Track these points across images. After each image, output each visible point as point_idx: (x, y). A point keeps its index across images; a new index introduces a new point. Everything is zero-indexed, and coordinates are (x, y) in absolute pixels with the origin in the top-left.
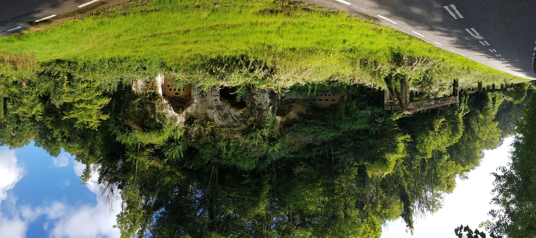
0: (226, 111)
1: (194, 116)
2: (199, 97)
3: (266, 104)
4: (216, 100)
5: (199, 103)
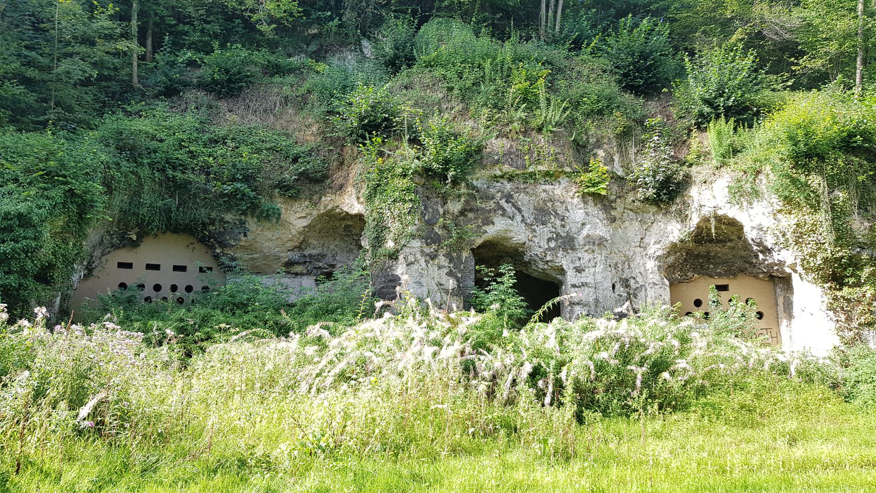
0: (544, 232)
3: (411, 259)
4: (579, 270)
5: (638, 259)
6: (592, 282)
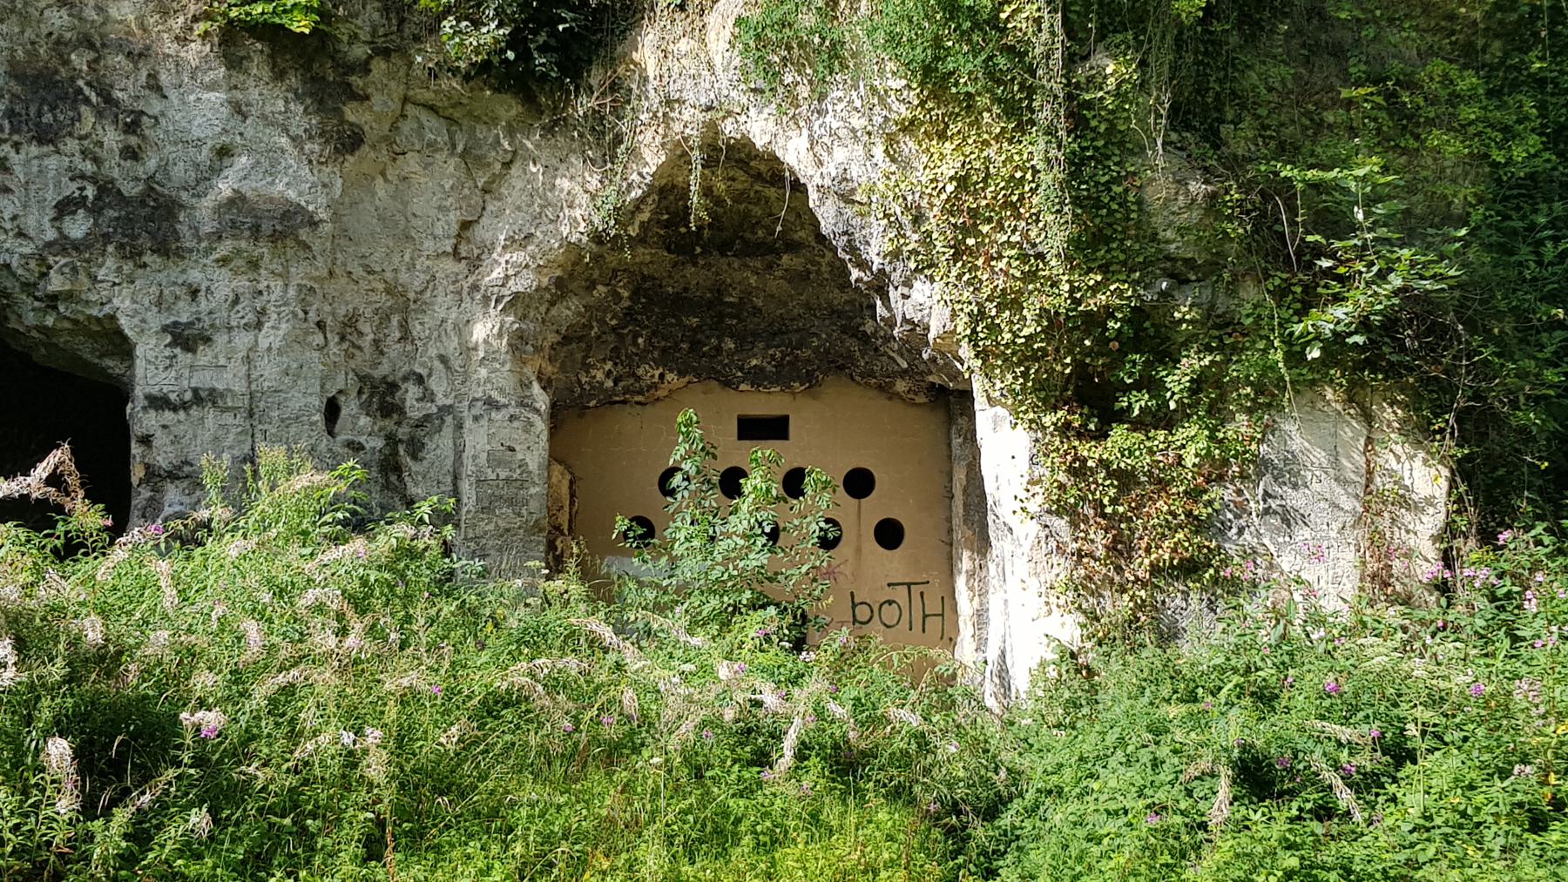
1: (509, 108)
2: (438, 385)
4: (185, 338)
5: (443, 306)
6: (239, 387)
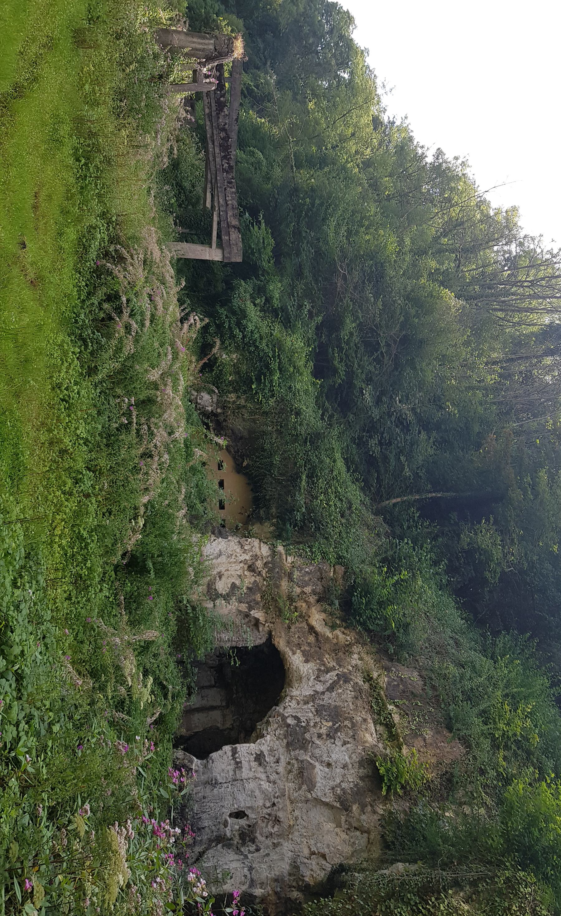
4: (259, 758)
